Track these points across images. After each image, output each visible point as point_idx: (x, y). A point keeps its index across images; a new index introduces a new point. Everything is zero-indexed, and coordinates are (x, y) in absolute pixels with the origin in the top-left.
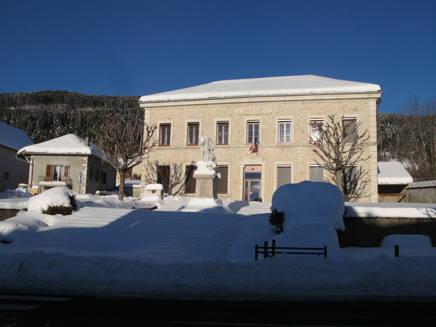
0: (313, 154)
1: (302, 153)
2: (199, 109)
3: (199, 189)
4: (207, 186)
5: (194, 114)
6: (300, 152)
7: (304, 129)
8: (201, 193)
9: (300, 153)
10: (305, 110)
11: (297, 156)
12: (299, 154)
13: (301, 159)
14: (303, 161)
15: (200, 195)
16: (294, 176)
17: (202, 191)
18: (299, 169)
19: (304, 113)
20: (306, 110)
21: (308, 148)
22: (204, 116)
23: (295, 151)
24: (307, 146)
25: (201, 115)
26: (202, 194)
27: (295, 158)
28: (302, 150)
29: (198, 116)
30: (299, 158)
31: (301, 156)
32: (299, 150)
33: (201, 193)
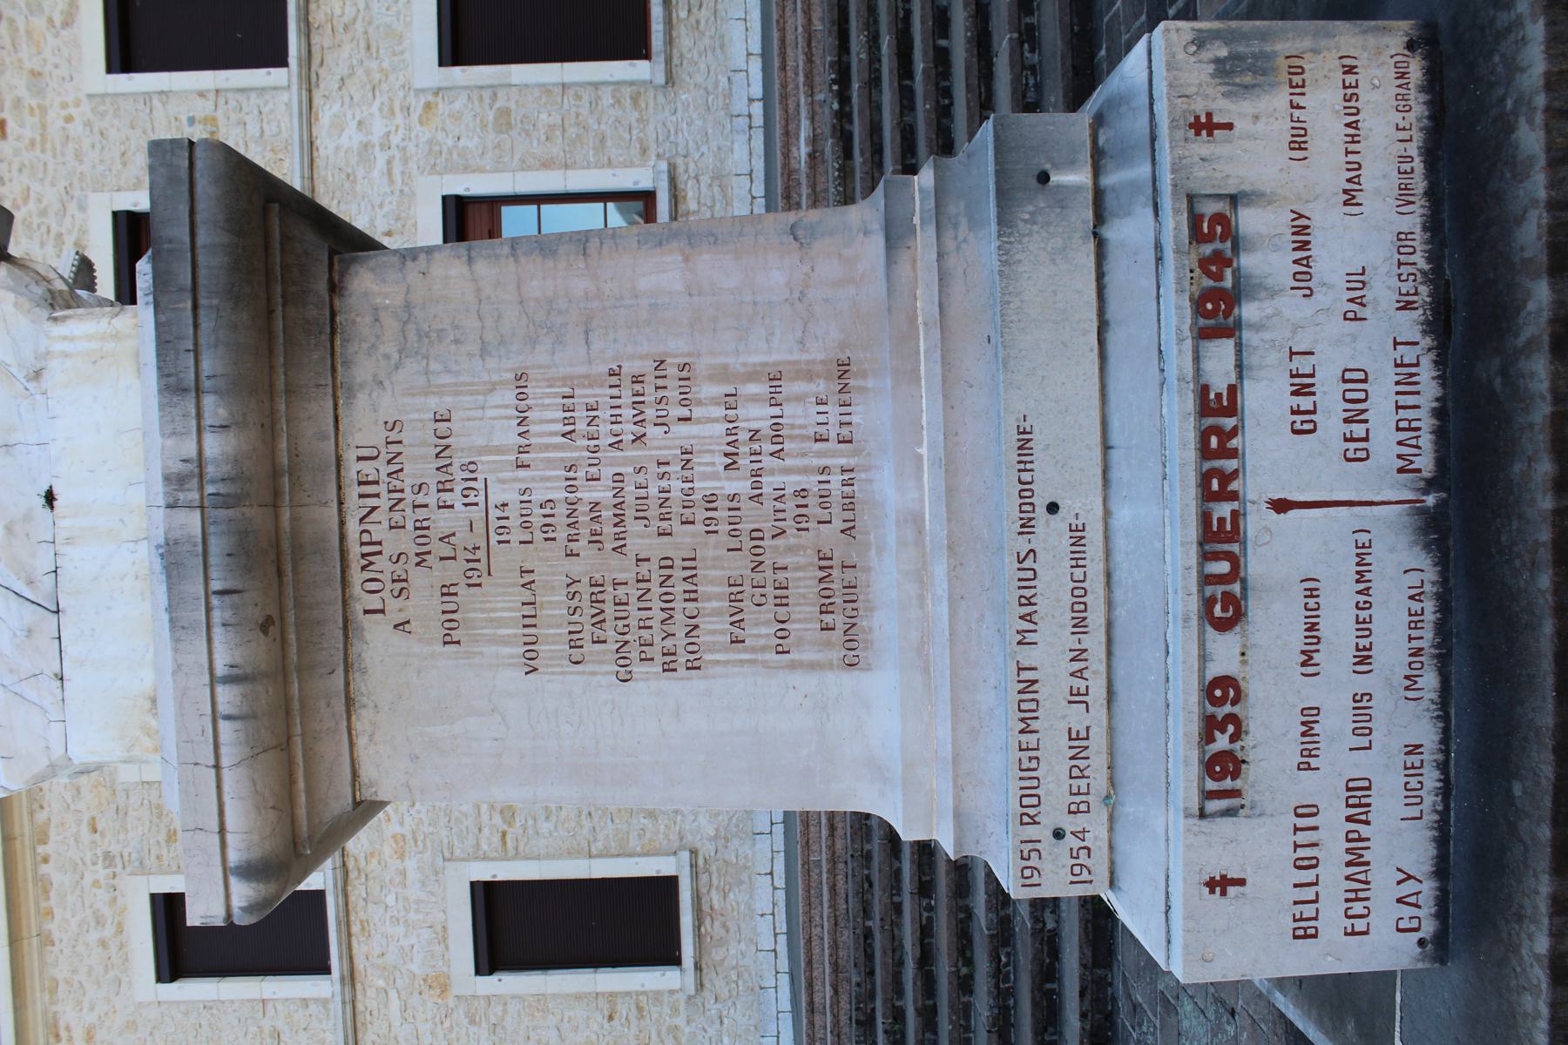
0: (368, 48)
1: (360, 123)
2: (53, 902)
3: (649, 685)
4: (547, 420)
5: (94, 936)
6: (351, 138)
7: (184, 119)
8: (760, 630)
9: (359, 138)
10: (52, 115)
11: (381, 159)
12: (366, 146)
13: (401, 131)
14: (415, 117)
15: (851, 640)
16: (524, 166)
17: (712, 587)
18: (469, 143)
19: (69, 119)
20: (44, 110)
21: (322, 86)
22: (108, 858)
23: (344, 176)
24: (310, 91)
25: (96, 884)
26: (804, 585)
27: (397, 171)
28: (338, 127)
29: (106, 911)
30: (396, 140)
31: (378, 127)
32: (337, 148)
33: (760, 630)
